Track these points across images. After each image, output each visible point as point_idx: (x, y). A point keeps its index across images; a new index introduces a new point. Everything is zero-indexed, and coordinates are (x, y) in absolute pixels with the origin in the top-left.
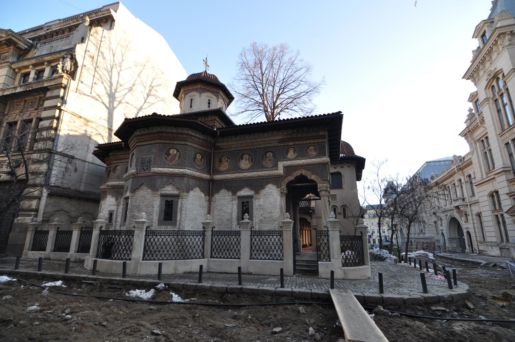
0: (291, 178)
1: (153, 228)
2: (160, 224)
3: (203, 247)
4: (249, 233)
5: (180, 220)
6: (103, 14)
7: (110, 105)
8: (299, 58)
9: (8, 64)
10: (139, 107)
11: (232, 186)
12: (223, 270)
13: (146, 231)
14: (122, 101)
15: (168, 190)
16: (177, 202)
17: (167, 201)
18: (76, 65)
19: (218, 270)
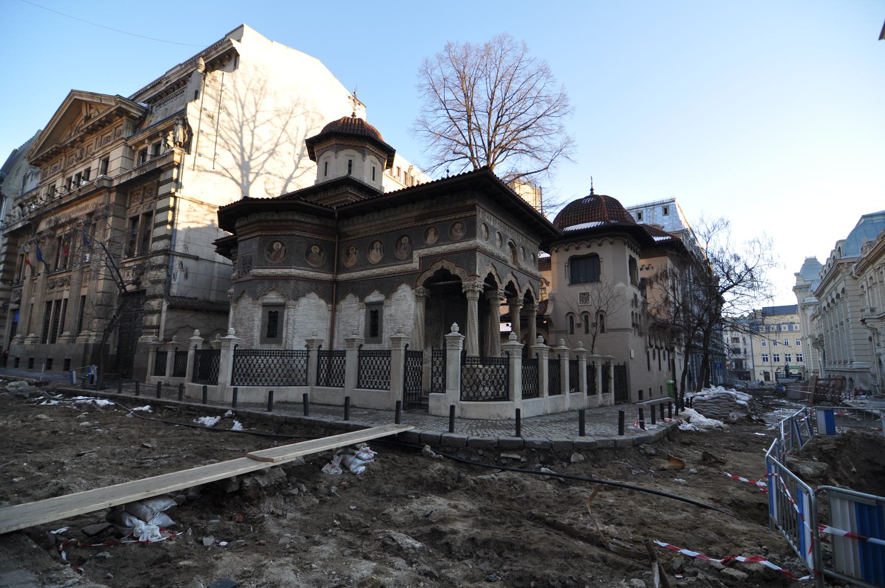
0: (429, 274)
1: (254, 348)
2: (263, 341)
3: (306, 371)
4: (356, 353)
5: (287, 337)
7: (243, 180)
8: (527, 56)
10: (286, 176)
11: (360, 288)
12: (326, 401)
13: (235, 350)
14: (261, 172)
17: (270, 312)
18: (190, 133)
19: (322, 401)
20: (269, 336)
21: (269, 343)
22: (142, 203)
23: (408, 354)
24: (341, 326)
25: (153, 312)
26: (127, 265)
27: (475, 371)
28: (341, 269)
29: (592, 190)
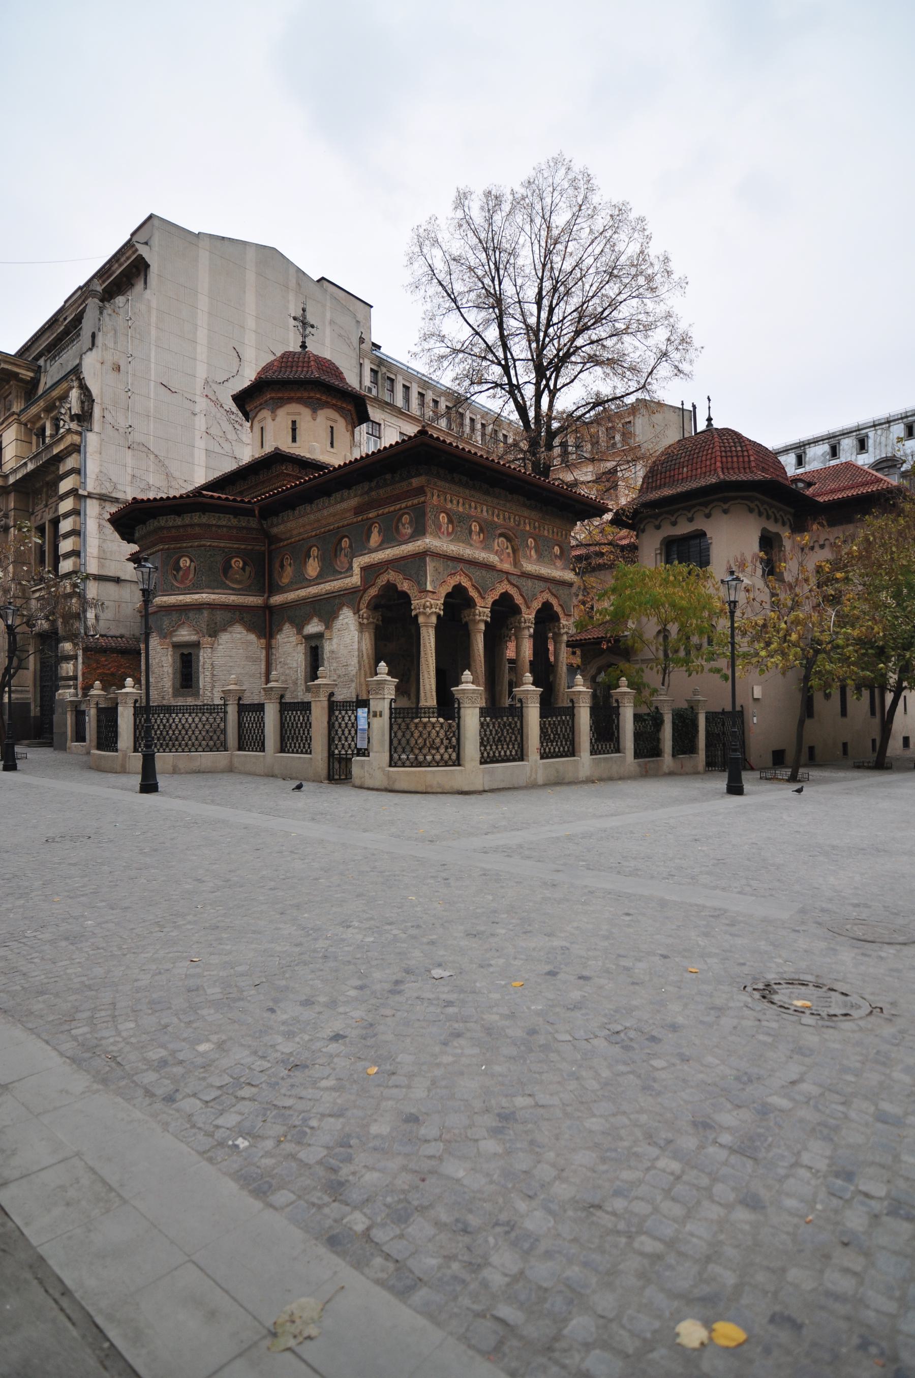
0: (373, 591)
1: (165, 702)
2: (176, 694)
3: (224, 731)
6: (128, 258)
9: (15, 416)
11: (297, 614)
15: (182, 636)
16: (198, 656)
17: (182, 654)
20: (183, 686)
21: (183, 695)
22: (46, 506)
23: (332, 706)
24: (280, 670)
25: (68, 658)
26: (37, 595)
27: (434, 728)
28: (273, 588)
29: (709, 419)
